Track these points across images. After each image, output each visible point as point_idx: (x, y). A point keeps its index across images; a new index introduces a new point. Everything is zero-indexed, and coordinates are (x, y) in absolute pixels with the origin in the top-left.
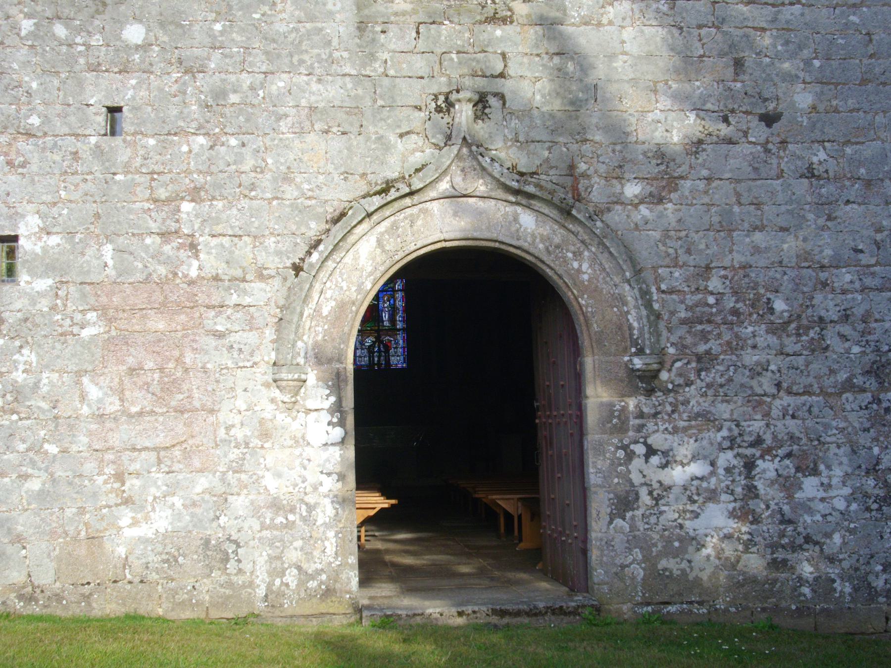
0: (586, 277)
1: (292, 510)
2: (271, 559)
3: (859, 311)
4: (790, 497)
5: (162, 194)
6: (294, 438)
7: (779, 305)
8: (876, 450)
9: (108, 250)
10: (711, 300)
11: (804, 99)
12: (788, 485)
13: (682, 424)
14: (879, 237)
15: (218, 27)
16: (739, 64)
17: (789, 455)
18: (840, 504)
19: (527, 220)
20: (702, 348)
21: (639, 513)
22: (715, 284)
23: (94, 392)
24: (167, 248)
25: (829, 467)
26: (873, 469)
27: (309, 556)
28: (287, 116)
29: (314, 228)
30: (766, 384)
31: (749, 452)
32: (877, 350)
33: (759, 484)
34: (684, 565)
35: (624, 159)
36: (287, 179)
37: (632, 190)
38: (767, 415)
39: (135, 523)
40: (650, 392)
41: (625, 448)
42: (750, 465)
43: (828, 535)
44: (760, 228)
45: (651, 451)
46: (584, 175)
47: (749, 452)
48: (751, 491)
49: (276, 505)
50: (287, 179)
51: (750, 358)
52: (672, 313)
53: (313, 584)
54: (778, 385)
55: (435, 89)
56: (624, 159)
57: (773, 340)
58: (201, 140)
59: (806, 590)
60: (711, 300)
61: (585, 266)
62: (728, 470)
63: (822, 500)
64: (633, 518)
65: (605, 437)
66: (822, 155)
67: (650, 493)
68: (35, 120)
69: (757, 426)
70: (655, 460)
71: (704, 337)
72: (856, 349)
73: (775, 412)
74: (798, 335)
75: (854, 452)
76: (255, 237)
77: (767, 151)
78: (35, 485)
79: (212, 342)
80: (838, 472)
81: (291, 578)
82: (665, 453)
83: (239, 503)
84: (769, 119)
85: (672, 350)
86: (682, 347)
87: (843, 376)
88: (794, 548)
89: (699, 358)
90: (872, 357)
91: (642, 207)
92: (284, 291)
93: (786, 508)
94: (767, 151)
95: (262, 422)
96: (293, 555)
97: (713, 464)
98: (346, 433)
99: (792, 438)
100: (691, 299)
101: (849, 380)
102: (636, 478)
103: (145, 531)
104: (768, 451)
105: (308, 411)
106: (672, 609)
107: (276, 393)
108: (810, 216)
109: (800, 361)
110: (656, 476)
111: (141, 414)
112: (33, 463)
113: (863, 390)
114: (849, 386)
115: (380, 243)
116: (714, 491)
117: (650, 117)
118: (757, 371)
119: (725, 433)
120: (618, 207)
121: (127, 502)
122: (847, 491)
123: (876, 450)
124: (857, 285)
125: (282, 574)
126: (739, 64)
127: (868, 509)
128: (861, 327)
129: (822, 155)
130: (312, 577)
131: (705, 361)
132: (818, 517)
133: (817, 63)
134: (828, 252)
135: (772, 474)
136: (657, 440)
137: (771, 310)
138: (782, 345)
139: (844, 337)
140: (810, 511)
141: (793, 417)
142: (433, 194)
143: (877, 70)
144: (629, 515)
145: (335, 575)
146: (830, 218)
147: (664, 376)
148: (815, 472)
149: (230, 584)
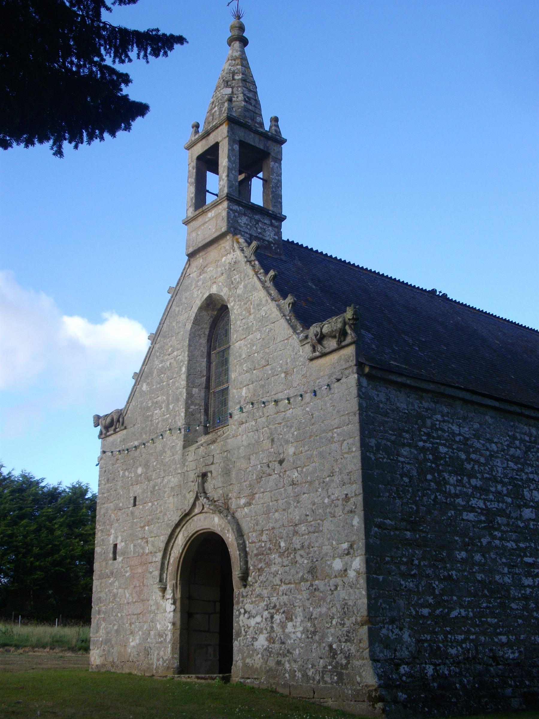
3: (306, 544)
7: (282, 544)
8: (311, 609)
11: (291, 450)
12: (283, 626)
13: (254, 599)
18: (299, 635)
25: (296, 618)
30: (277, 581)
31: (272, 611)
32: (312, 561)
33: (274, 626)
34: (253, 662)
42: (272, 617)
43: (295, 650)
46: (230, 499)
47: (272, 611)
51: (274, 569)
52: (252, 552)
54: (281, 580)
59: (287, 675)
60: (263, 545)
63: (294, 633)
66: (296, 474)
70: (246, 615)
71: (260, 561)
72: (306, 562)
73: (280, 593)
74: (288, 557)
75: (304, 610)
77: (280, 476)
80: (299, 620)
87: (301, 574)
89: (259, 570)
90: (310, 565)
93: (282, 636)
94: (280, 476)
96: (162, 653)
98: (176, 607)
99: (285, 604)
101: (303, 576)
106: (249, 681)
108: (292, 502)
110: (247, 622)
111: (135, 602)
113: (307, 581)
114: (303, 579)
116: (262, 629)
118: (275, 574)
119: (265, 603)
120: (239, 509)
122: (301, 629)
123: (311, 609)
124: (306, 532)
127: (308, 637)
128: (307, 550)
132: (292, 641)
134: (298, 518)
138: (283, 562)
139: (301, 556)
140: (290, 638)
141: (286, 595)
143: (315, 430)
146: (298, 502)
148: (291, 620)
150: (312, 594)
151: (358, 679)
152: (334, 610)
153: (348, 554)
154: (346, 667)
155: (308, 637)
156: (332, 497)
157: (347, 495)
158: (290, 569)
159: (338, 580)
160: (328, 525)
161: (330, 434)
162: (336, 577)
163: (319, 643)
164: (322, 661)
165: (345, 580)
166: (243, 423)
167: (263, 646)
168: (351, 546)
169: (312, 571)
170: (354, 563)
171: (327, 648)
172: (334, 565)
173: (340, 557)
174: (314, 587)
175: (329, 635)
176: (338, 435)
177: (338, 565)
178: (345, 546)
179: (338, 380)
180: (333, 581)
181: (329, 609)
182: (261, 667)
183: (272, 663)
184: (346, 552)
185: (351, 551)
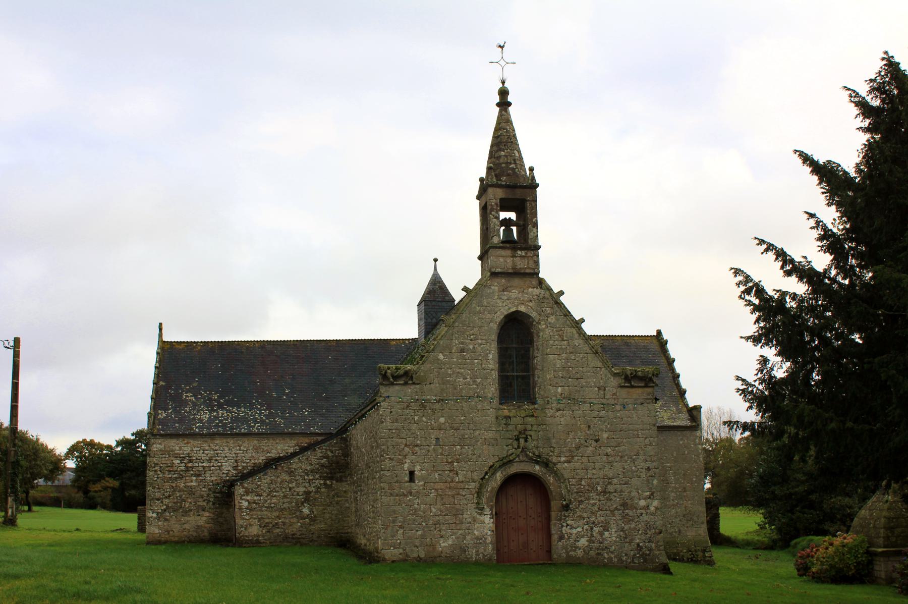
0: (551, 481)
1: (481, 539)
2: (476, 551)
3: (619, 490)
4: (602, 537)
5: (450, 461)
6: (481, 521)
7: (599, 488)
9: (436, 475)
10: (582, 487)
11: (605, 435)
12: (601, 534)
14: (624, 471)
15: (462, 418)
16: (589, 427)
17: (601, 526)
19: (537, 467)
20: (580, 499)
21: (564, 540)
22: (583, 483)
23: (434, 510)
24: (451, 474)
25: (611, 529)
26: (622, 530)
27: (485, 550)
28: (479, 441)
29: (486, 469)
30: (596, 508)
31: (591, 525)
32: (623, 500)
33: (594, 534)
35: (561, 451)
36: (480, 457)
37: (563, 459)
38: (596, 516)
39: (444, 542)
40: (567, 511)
41: (561, 524)
42: (592, 529)
43: (611, 546)
44: (595, 469)
45: (567, 525)
47: (591, 525)
48: (592, 536)
49: (478, 538)
50: (480, 457)
51: (592, 502)
53: (486, 557)
54: (599, 509)
55: (515, 434)
56: (561, 451)
57: (598, 497)
58: (459, 447)
61: (551, 478)
62: (587, 530)
63: (610, 537)
64: (563, 542)
65: (556, 522)
66: (610, 450)
67: (567, 536)
68: (419, 442)
69: (593, 519)
70: (568, 527)
71: (581, 496)
74: (604, 496)
75: (618, 526)
76: (471, 471)
78: (420, 533)
79: (462, 497)
80: (613, 530)
81: (481, 556)
82: (571, 526)
83: (468, 537)
84: (597, 441)
85: (572, 500)
86: (575, 499)
87: (615, 506)
88: (603, 550)
89: (579, 501)
91: (565, 464)
92: (479, 485)
94: (596, 449)
95: (474, 517)
96: (482, 550)
97: (583, 528)
99: (602, 522)
100: (577, 487)
101: (616, 507)
102: (564, 532)
103: (446, 544)
104: (596, 525)
105: (485, 515)
107: (477, 510)
108: (607, 466)
109: (604, 502)
112: (419, 528)
113: (620, 510)
114: (616, 509)
115: (502, 473)
117: (567, 441)
118: (594, 505)
121: (442, 537)
122: (616, 535)
125: (479, 555)
126: (589, 427)
127: (621, 540)
129: (610, 450)
130: (486, 556)
131: (581, 502)
132: (609, 542)
133: (609, 426)
135: (597, 531)
136: (569, 522)
137: (597, 490)
138: (600, 499)
139: (615, 497)
140: (607, 540)
141: (602, 516)
142: (515, 461)
144: (562, 541)
145: (491, 556)
146: (612, 466)
147: (571, 506)
148: (608, 531)
149: (466, 558)
150: (623, 517)
151: (657, 561)
152: (640, 526)
153: (650, 498)
154: (649, 555)
155: (621, 540)
156: (639, 467)
157: (648, 467)
158: (606, 503)
159: (643, 511)
160: (635, 481)
161: (636, 432)
162: (641, 509)
163: (630, 543)
164: (632, 552)
165: (648, 511)
166: (560, 410)
167: (584, 545)
168: (652, 494)
169: (624, 505)
170: (654, 503)
171: (636, 546)
172: (639, 503)
173: (645, 499)
174: (625, 513)
175: (637, 538)
176: (642, 434)
177: (642, 503)
178: (648, 493)
179: (642, 404)
180: (639, 511)
181: (636, 525)
182: (583, 557)
183: (592, 553)
184: (648, 497)
185: (652, 497)
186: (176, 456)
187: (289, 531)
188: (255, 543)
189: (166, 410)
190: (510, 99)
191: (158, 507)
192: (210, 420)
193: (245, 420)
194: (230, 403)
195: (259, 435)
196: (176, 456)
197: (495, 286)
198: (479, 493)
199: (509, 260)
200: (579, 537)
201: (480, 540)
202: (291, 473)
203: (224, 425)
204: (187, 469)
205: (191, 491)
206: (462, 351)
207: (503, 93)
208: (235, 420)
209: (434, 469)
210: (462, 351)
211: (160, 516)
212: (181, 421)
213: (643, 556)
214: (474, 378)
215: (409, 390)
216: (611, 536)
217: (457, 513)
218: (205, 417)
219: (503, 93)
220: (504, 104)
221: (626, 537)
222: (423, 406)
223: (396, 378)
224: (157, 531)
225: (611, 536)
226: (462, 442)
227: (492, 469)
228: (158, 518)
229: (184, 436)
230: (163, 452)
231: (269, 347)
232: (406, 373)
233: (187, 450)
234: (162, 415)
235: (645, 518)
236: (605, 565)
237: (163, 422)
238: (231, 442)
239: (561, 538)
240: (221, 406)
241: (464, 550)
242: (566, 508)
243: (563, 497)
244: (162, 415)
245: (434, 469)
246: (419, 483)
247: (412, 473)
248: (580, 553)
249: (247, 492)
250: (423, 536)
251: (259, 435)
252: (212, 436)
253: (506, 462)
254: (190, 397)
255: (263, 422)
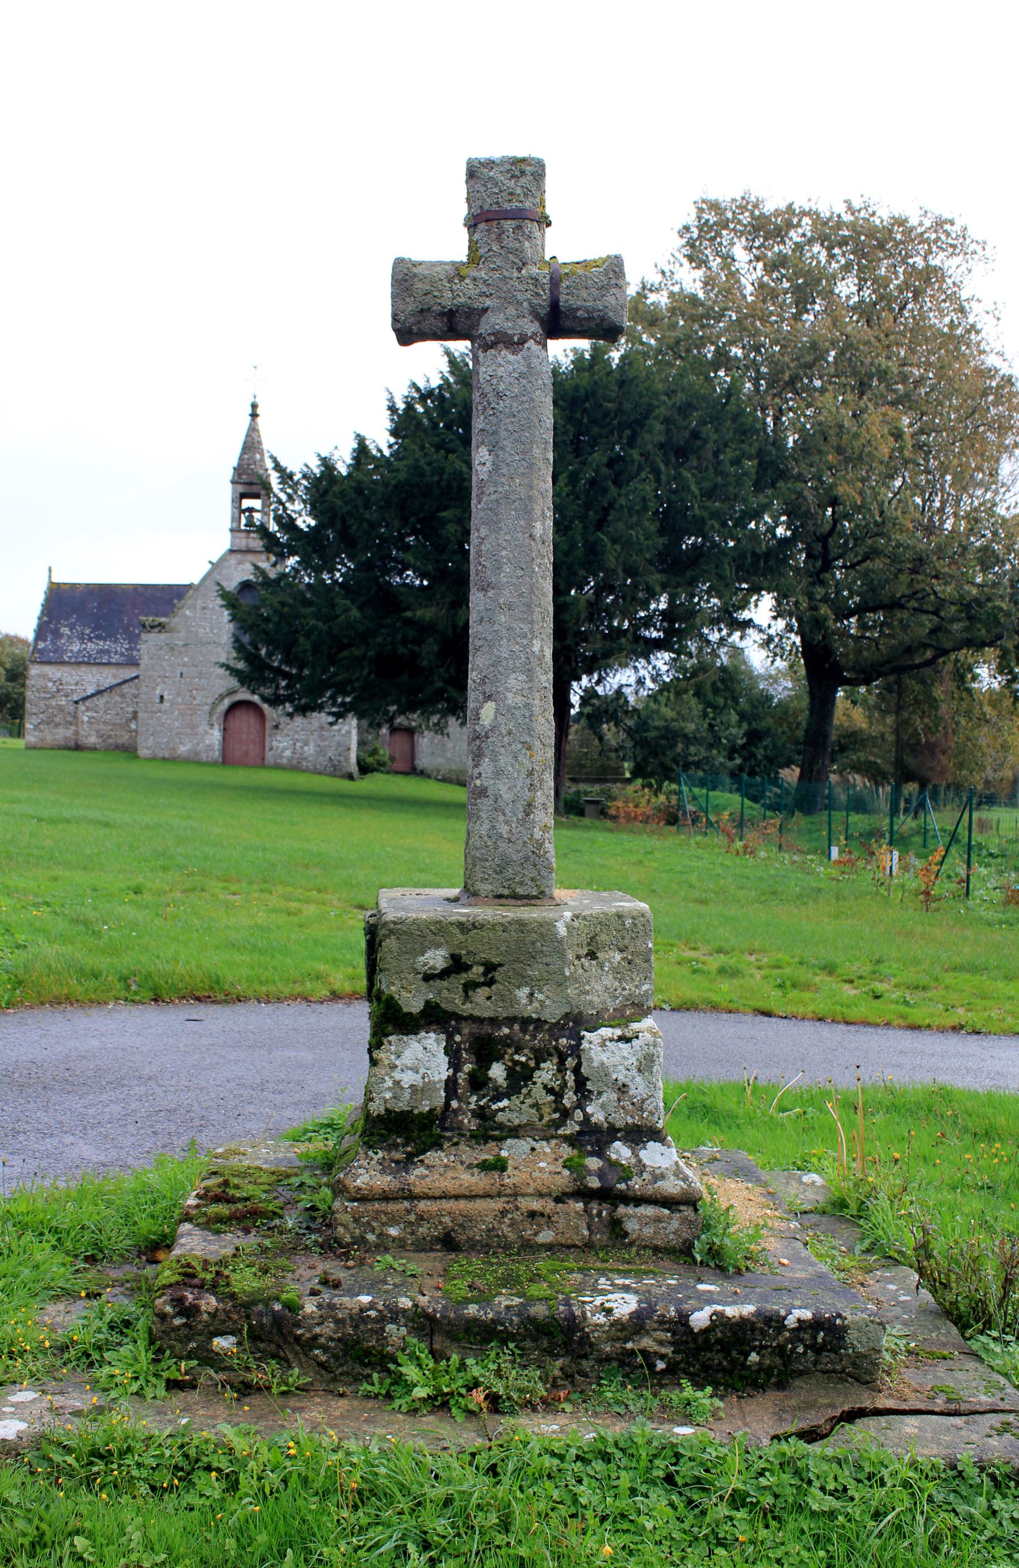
12: (302, 748)
186: (50, 680)
187: (120, 741)
188: (93, 749)
189: (45, 641)
190: (259, 412)
191: (35, 720)
192: (80, 651)
193: (108, 652)
194: (99, 637)
195: (117, 664)
196: (50, 680)
197: (233, 560)
198: (211, 714)
199: (244, 541)
200: (285, 749)
201: (210, 747)
202: (123, 696)
203: (90, 656)
204: (59, 691)
205: (61, 709)
206: (204, 608)
207: (254, 406)
208: (101, 652)
209: (178, 694)
210: (204, 608)
211: (36, 727)
212: (55, 651)
213: (334, 766)
214: (212, 629)
215: (163, 636)
216: (310, 750)
217: (194, 727)
218: (76, 647)
219: (254, 406)
220: (254, 415)
221: (321, 751)
222: (172, 649)
223: (152, 627)
224: (33, 739)
225: (310, 750)
226: (200, 676)
227: (222, 698)
228: (34, 730)
229: (56, 663)
230: (39, 676)
231: (141, 590)
232: (160, 624)
233: (58, 675)
234: (41, 645)
235: (337, 738)
236: (303, 771)
237: (41, 652)
238: (94, 669)
239: (271, 749)
240: (90, 639)
241: (197, 754)
242: (276, 727)
243: (273, 720)
244: (41, 645)
245: (178, 694)
246: (166, 704)
247: (162, 697)
248: (284, 761)
249: (88, 709)
250: (168, 742)
251: (117, 664)
252: (79, 664)
253: (231, 692)
254: (65, 631)
255: (122, 654)
